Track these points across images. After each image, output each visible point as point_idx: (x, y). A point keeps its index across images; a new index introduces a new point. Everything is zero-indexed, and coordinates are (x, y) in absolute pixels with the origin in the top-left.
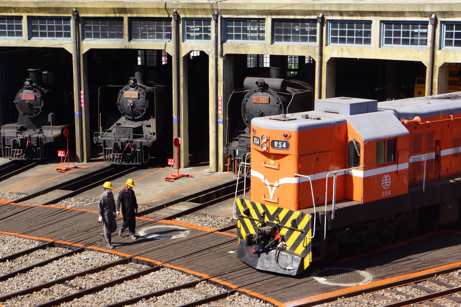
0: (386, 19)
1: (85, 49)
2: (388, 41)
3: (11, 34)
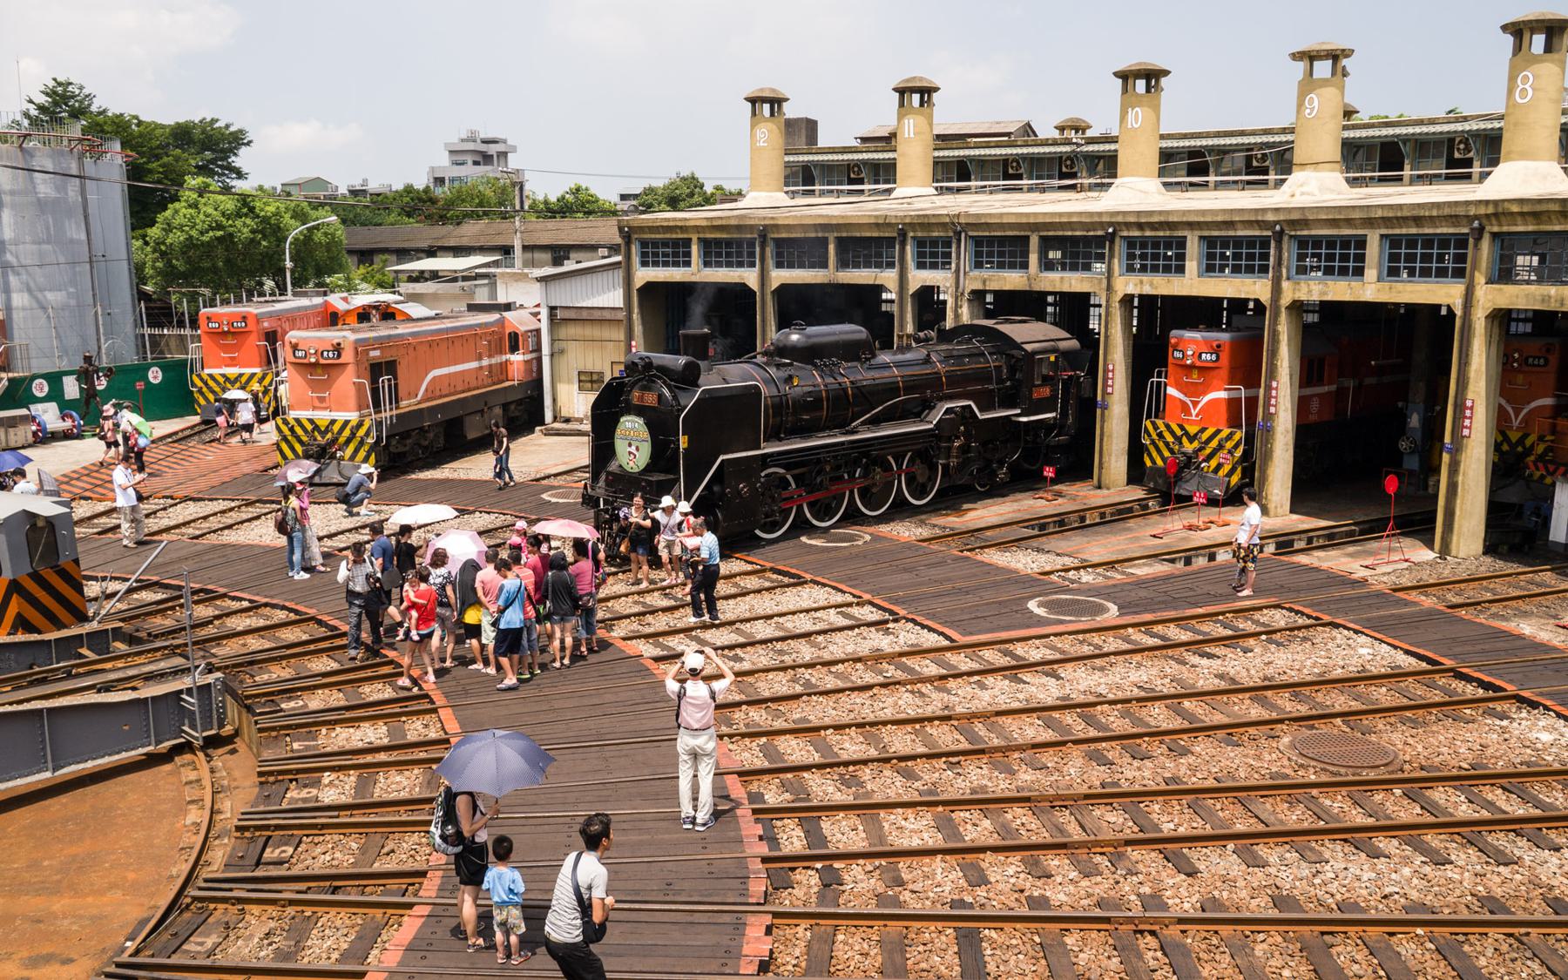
0: (1206, 233)
1: (775, 285)
2: (1210, 269)
3: (676, 264)
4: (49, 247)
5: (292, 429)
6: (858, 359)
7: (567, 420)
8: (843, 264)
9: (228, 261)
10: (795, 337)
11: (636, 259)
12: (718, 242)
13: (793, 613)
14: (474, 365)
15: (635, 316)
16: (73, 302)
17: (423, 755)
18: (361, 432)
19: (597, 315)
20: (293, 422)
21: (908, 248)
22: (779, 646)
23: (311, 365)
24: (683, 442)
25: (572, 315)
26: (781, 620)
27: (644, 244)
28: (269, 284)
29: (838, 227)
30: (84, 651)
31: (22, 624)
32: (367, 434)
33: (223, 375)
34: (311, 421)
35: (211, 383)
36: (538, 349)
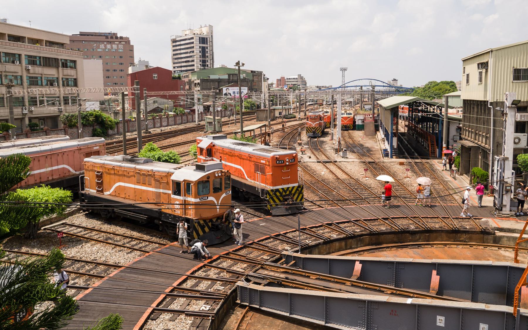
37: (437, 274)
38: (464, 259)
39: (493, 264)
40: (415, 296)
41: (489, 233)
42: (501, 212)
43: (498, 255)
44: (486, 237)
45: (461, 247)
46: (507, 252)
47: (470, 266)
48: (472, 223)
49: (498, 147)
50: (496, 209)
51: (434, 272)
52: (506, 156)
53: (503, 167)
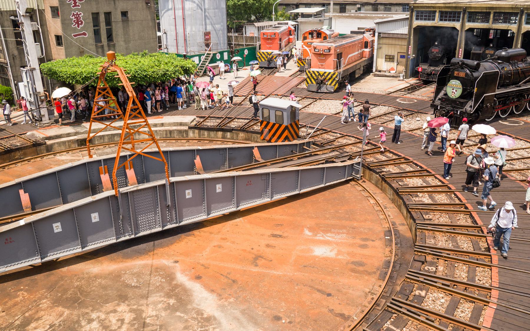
1: (467, 28)
3: (429, 20)
4: (217, 10)
5: (311, 75)
6: (522, 61)
7: (380, 71)
8: (495, 21)
9: (245, 10)
10: (503, 53)
11: (414, 18)
12: (446, 13)
13: (519, 149)
14: (357, 53)
15: (412, 37)
16: (222, 28)
17: (440, 190)
18: (334, 76)
19: (395, 36)
20: (311, 72)
21: (524, 17)
22: (523, 160)
23: (320, 54)
24: (475, 90)
25: (386, 36)
26: (516, 151)
27: (418, 12)
28: (253, 18)
29: (496, 8)
30: (305, 147)
31: (287, 138)
32: (336, 77)
33: (267, 52)
34: (318, 72)
35: (263, 55)
36: (372, 47)
37: (25, 192)
38: (30, 174)
39: (74, 165)
40: (14, 219)
41: (40, 145)
42: (41, 122)
43: (57, 161)
44: (38, 148)
45: (19, 164)
46: (63, 156)
47: (54, 174)
48: (19, 139)
49: (19, 59)
50: (36, 120)
51: (21, 192)
52: (32, 67)
53: (32, 78)
